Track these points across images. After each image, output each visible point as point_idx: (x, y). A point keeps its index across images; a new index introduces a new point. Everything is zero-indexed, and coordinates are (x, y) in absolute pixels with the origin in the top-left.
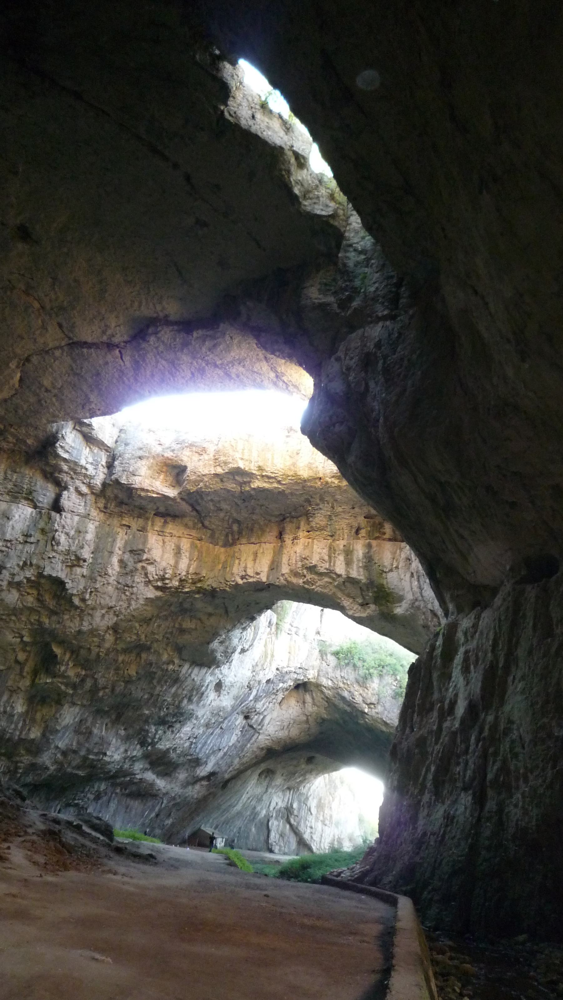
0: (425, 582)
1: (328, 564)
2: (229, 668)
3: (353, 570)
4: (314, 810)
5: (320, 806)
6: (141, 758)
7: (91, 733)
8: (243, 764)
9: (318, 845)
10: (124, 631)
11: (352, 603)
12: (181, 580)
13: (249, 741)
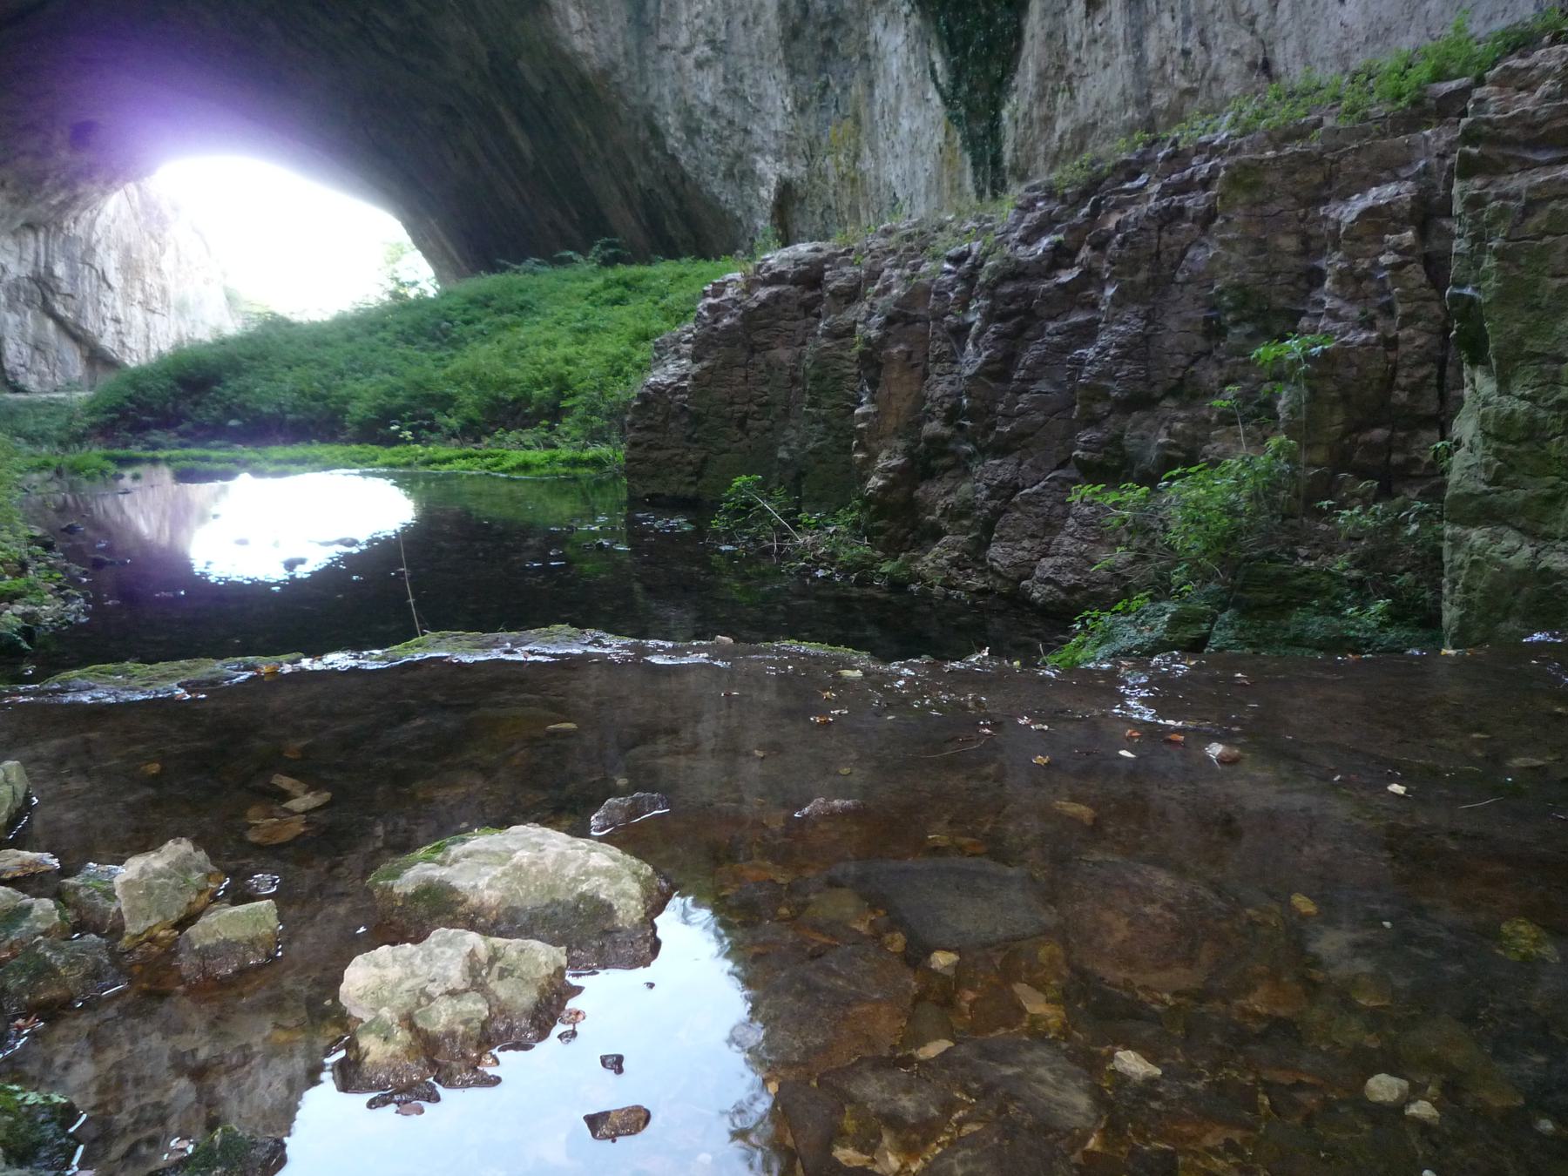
4: (114, 278)
5: (131, 268)
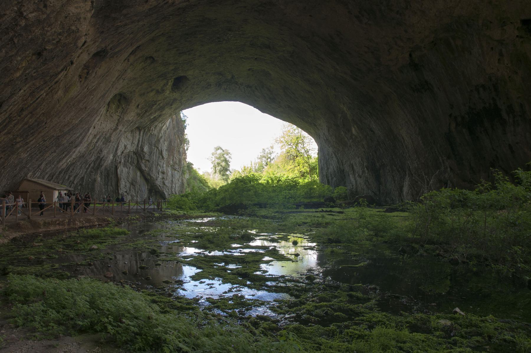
4: (165, 154)
9: (170, 190)
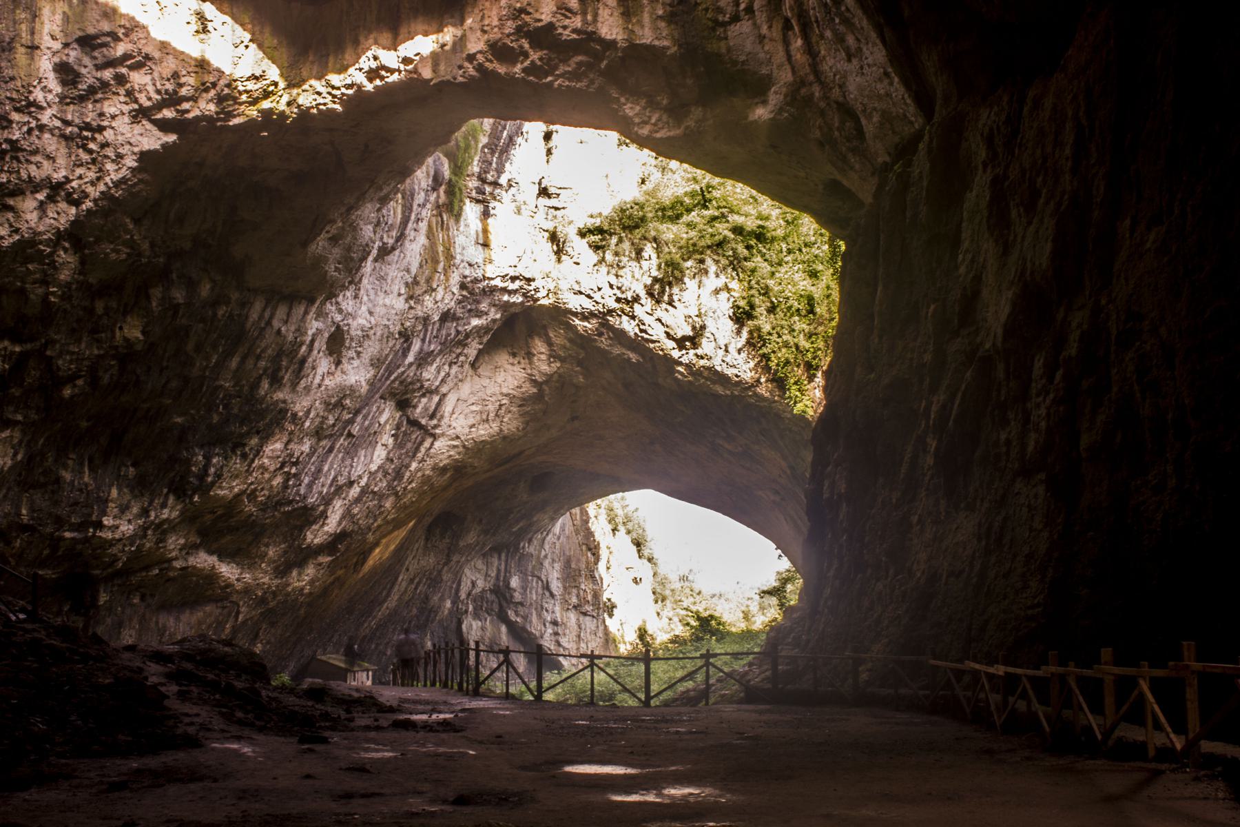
0: (822, 37)
1: (579, 18)
2: (356, 297)
3: (643, 27)
4: (556, 586)
6: (180, 523)
7: (58, 480)
8: (405, 507)
10: (98, 240)
11: (645, 108)
12: (220, 99)
13: (414, 456)
